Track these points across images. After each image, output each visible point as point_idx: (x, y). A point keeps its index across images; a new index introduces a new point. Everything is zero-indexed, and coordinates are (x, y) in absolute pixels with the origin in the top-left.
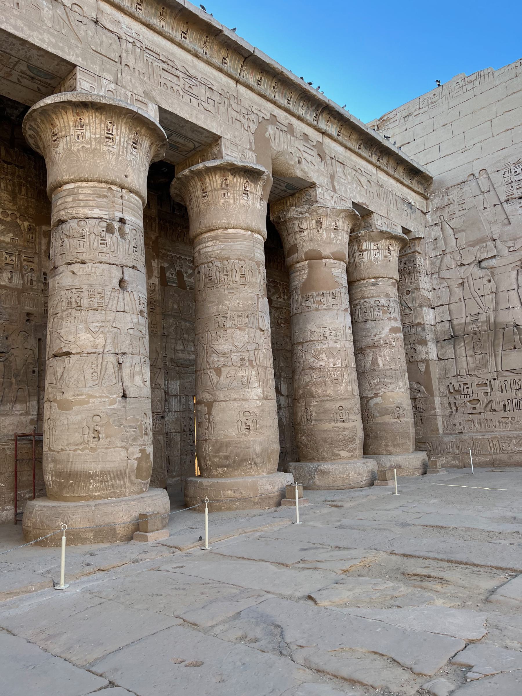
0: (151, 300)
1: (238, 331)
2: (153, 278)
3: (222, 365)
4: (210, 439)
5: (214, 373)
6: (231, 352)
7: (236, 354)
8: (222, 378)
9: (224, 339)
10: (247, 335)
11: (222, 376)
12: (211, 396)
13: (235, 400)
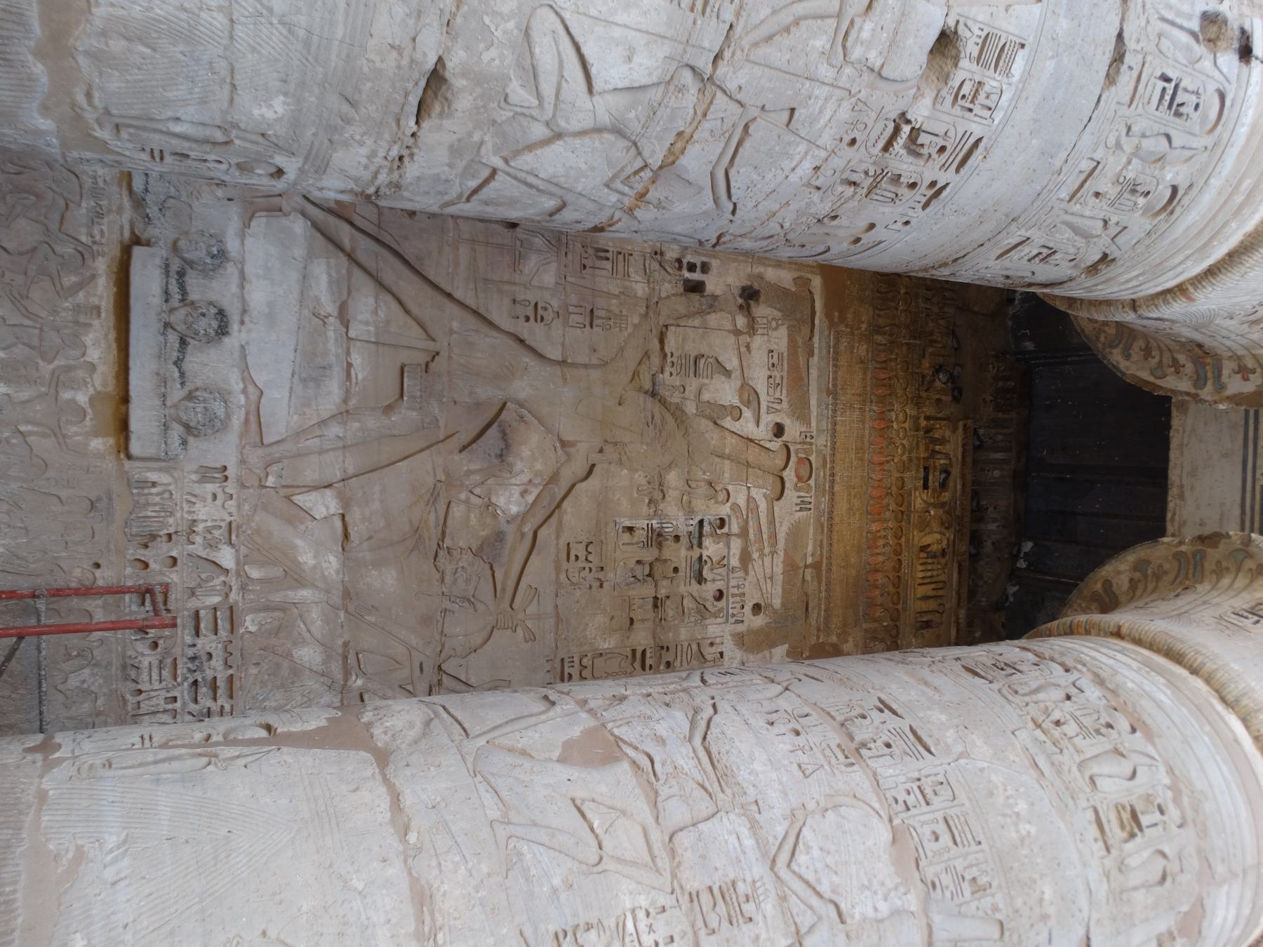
0: (672, 649)
1: (885, 835)
2: (739, 654)
3: (645, 762)
4: (49, 766)
5: (575, 732)
6: (752, 811)
7: (749, 842)
8: (563, 772)
9: (804, 759)
10: (884, 908)
11: (574, 773)
12: (412, 734)
13: (422, 898)
